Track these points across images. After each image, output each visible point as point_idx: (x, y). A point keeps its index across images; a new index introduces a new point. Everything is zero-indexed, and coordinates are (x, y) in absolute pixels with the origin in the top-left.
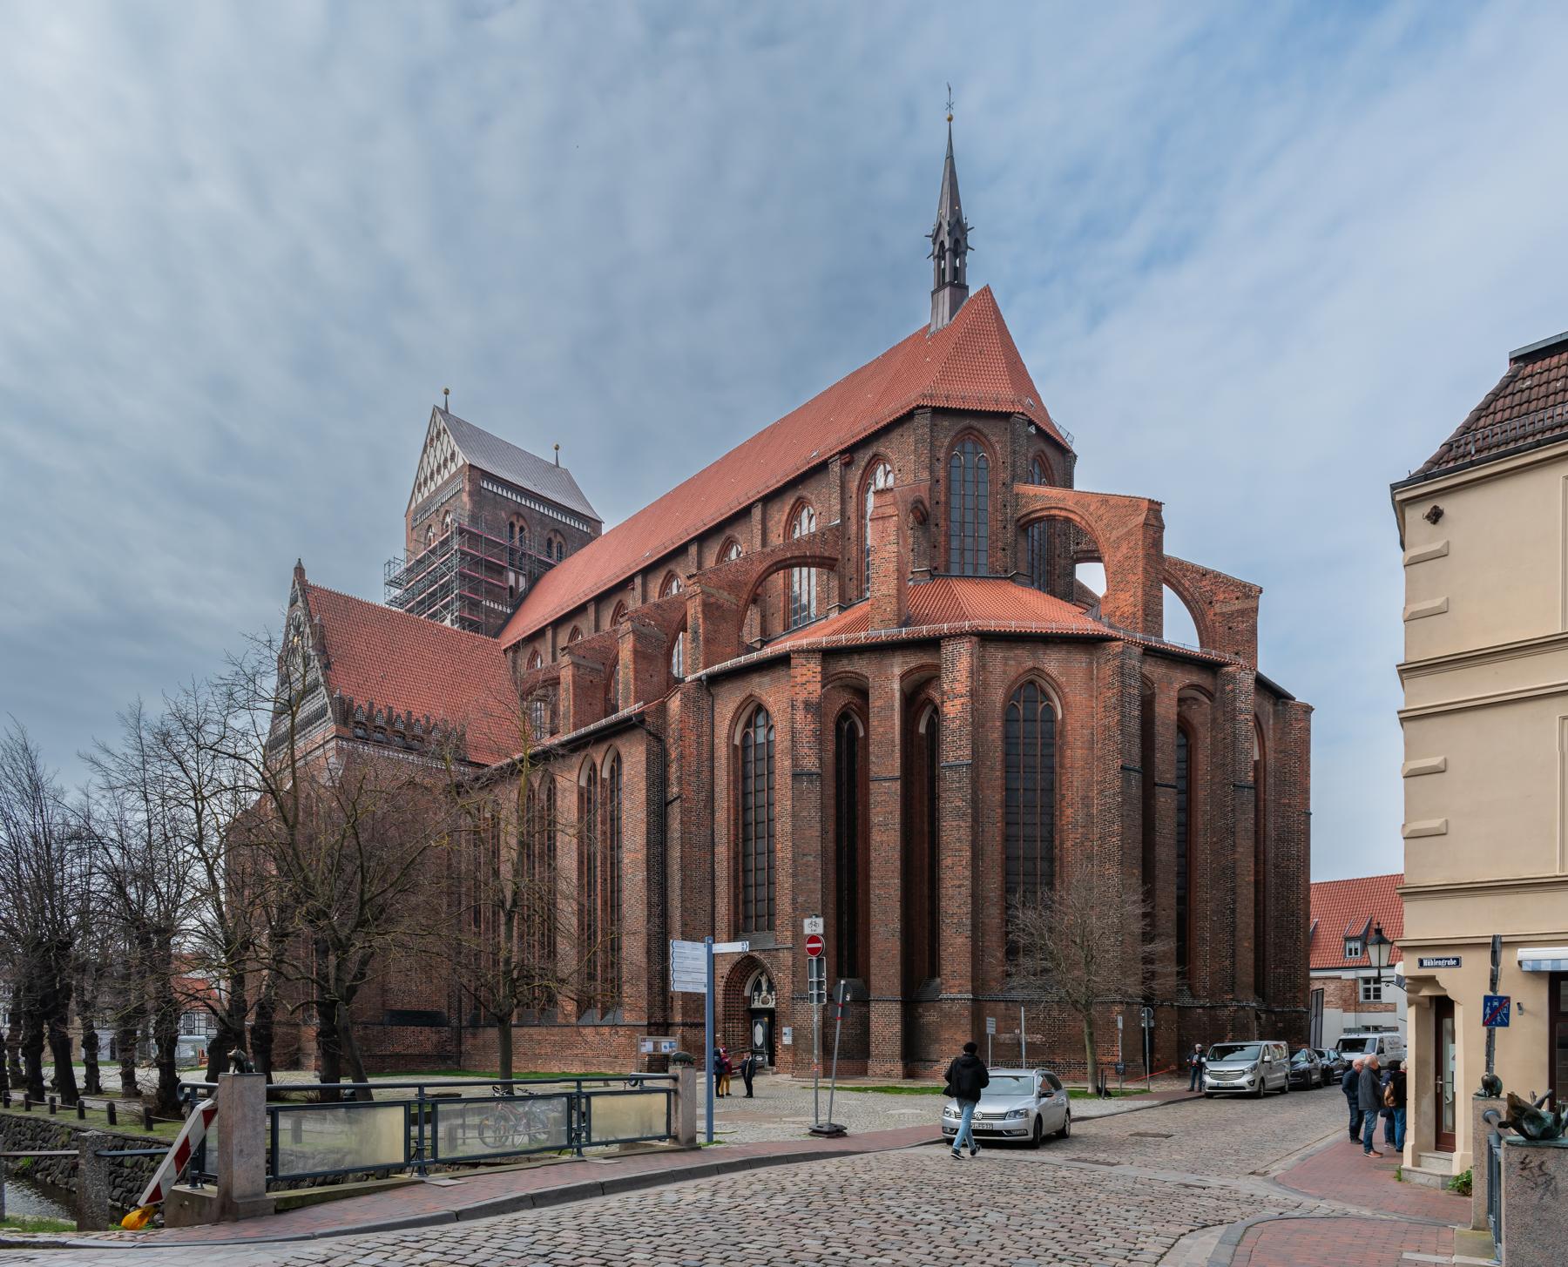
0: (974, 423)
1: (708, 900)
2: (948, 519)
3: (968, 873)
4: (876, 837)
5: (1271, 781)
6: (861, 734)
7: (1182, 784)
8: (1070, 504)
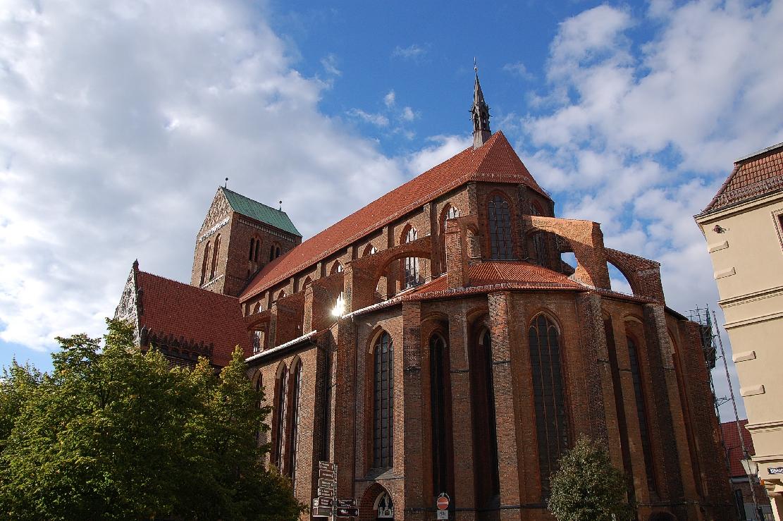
0: (499, 188)
4: (456, 407)
5: (684, 365)
6: (445, 346)
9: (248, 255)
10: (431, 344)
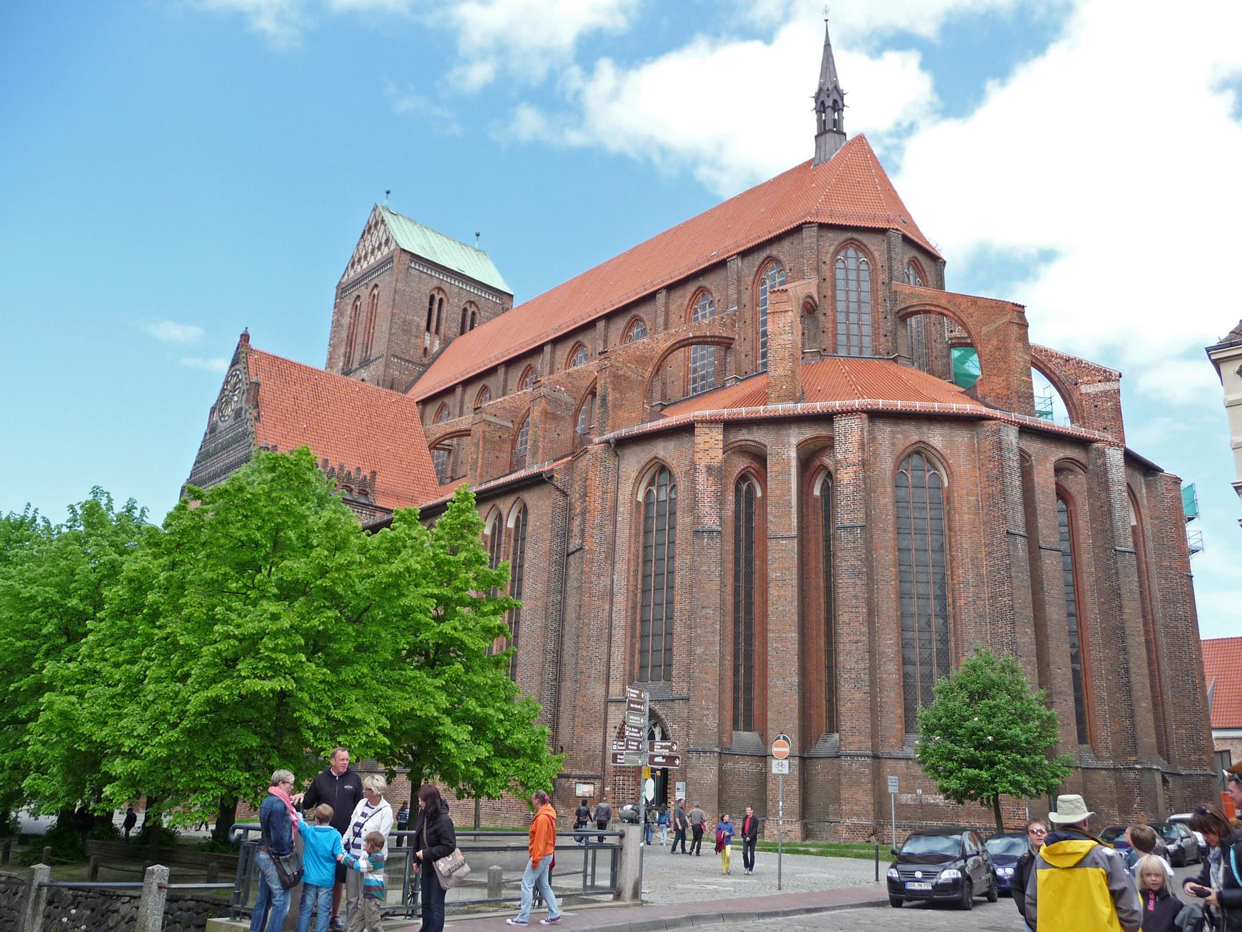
0: (856, 236)
1: (604, 648)
2: (834, 310)
3: (865, 629)
4: (773, 592)
5: (1150, 545)
6: (759, 494)
7: (1065, 546)
8: (943, 302)
9: (424, 324)
10: (738, 490)
